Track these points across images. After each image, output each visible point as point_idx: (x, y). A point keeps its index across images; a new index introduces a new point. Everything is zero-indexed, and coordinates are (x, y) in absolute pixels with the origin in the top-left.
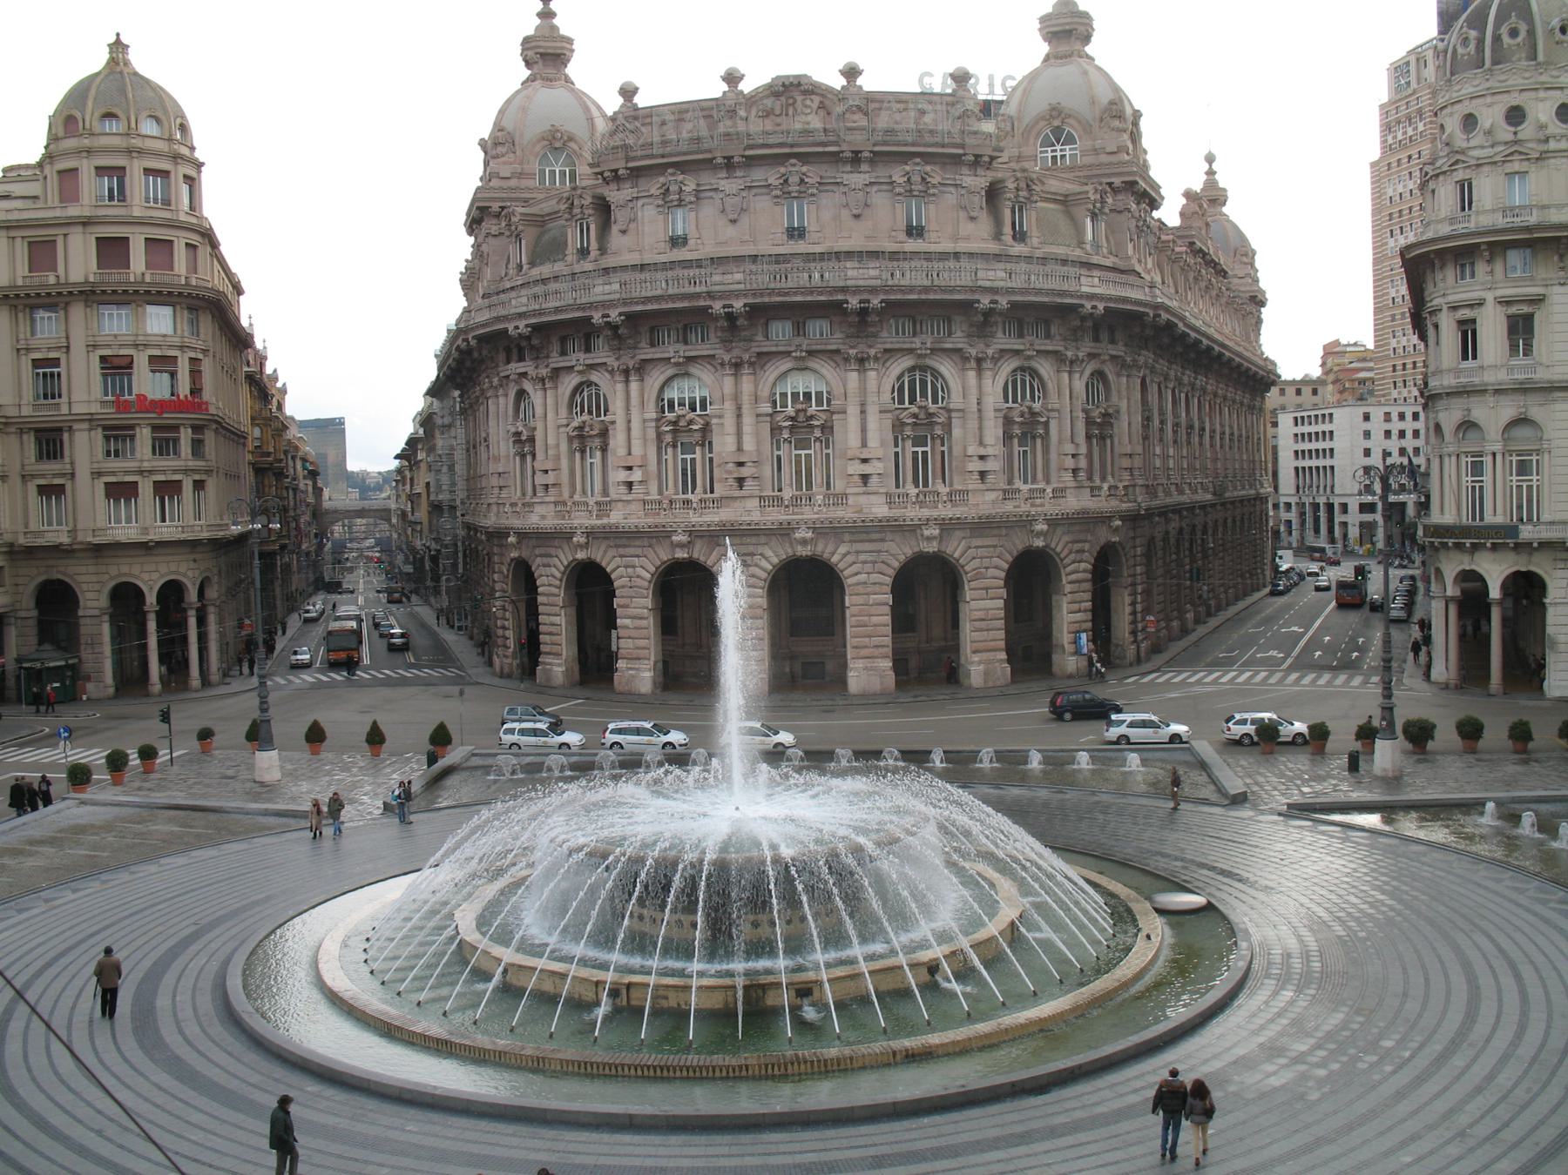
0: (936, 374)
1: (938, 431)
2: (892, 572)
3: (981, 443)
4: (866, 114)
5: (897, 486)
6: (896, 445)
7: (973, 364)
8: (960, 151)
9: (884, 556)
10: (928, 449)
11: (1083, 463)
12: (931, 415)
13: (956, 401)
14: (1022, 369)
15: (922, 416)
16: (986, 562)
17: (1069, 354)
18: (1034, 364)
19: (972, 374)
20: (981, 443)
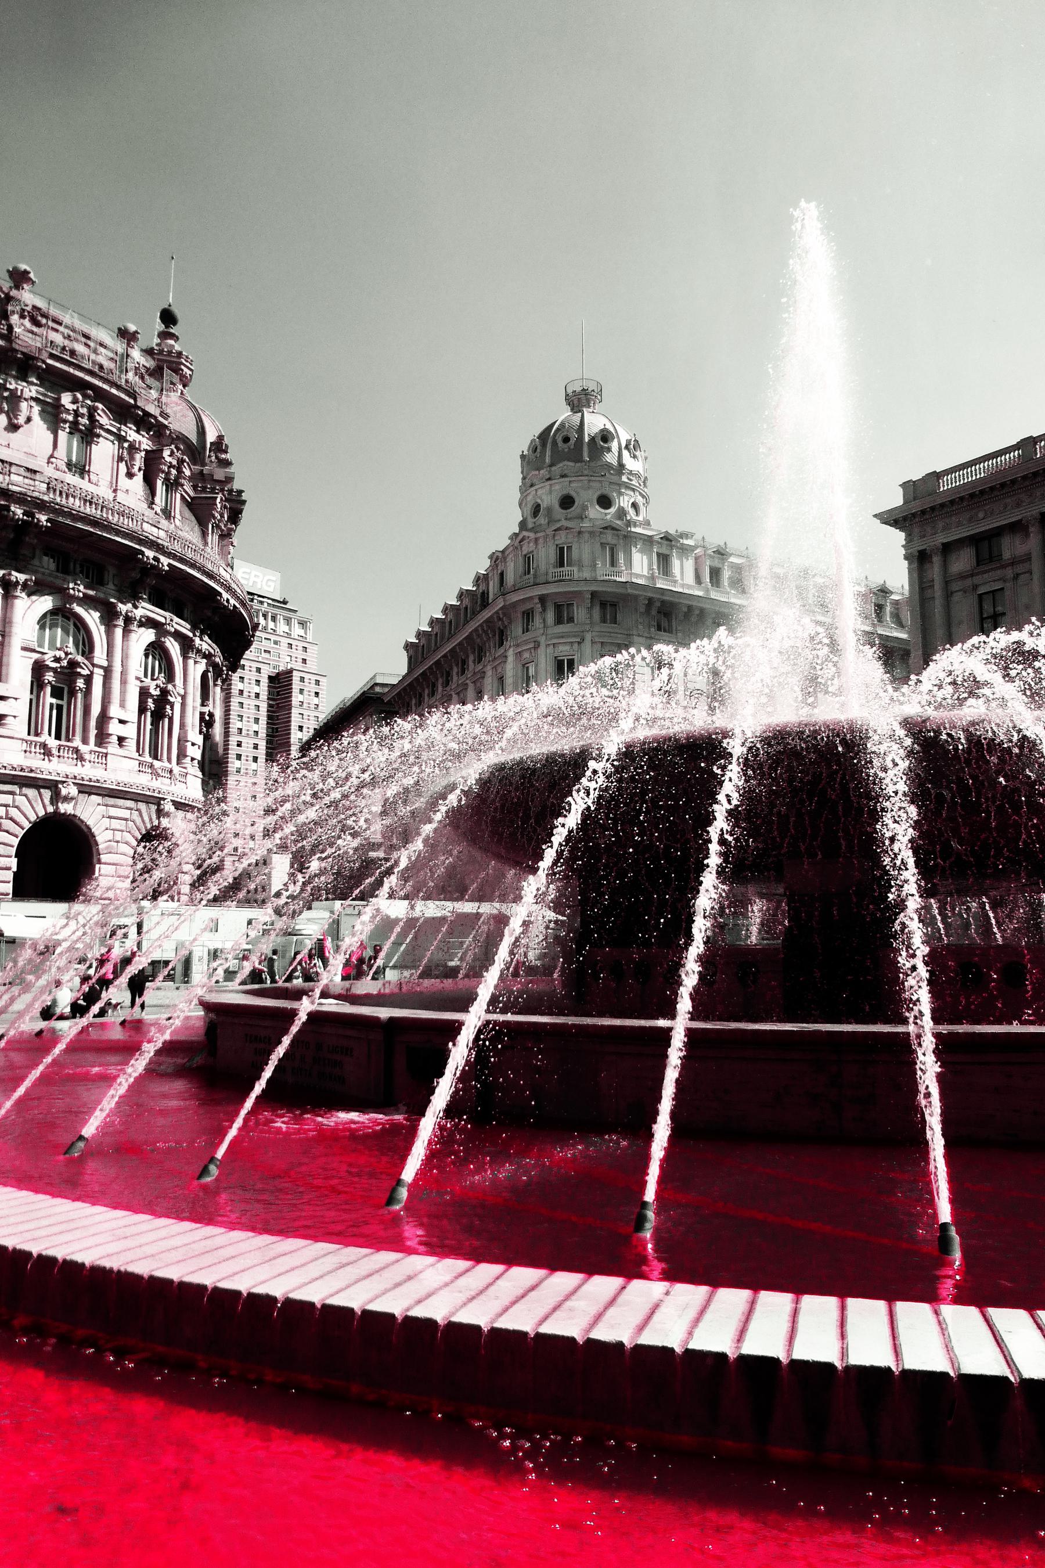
0: (81, 626)
1: (80, 683)
2: (21, 833)
3: (122, 705)
4: (38, 324)
5: (29, 734)
6: (32, 693)
7: (121, 622)
8: (132, 401)
9: (14, 812)
10: (64, 703)
11: (199, 757)
12: (73, 664)
13: (100, 655)
14: (152, 645)
15: (65, 663)
16: (118, 836)
17: (197, 641)
18: (168, 644)
19: (119, 632)
20: (122, 705)
